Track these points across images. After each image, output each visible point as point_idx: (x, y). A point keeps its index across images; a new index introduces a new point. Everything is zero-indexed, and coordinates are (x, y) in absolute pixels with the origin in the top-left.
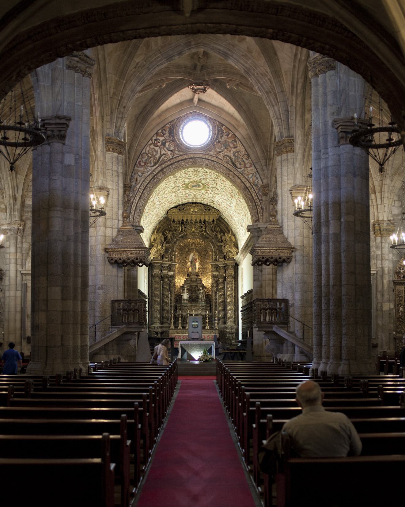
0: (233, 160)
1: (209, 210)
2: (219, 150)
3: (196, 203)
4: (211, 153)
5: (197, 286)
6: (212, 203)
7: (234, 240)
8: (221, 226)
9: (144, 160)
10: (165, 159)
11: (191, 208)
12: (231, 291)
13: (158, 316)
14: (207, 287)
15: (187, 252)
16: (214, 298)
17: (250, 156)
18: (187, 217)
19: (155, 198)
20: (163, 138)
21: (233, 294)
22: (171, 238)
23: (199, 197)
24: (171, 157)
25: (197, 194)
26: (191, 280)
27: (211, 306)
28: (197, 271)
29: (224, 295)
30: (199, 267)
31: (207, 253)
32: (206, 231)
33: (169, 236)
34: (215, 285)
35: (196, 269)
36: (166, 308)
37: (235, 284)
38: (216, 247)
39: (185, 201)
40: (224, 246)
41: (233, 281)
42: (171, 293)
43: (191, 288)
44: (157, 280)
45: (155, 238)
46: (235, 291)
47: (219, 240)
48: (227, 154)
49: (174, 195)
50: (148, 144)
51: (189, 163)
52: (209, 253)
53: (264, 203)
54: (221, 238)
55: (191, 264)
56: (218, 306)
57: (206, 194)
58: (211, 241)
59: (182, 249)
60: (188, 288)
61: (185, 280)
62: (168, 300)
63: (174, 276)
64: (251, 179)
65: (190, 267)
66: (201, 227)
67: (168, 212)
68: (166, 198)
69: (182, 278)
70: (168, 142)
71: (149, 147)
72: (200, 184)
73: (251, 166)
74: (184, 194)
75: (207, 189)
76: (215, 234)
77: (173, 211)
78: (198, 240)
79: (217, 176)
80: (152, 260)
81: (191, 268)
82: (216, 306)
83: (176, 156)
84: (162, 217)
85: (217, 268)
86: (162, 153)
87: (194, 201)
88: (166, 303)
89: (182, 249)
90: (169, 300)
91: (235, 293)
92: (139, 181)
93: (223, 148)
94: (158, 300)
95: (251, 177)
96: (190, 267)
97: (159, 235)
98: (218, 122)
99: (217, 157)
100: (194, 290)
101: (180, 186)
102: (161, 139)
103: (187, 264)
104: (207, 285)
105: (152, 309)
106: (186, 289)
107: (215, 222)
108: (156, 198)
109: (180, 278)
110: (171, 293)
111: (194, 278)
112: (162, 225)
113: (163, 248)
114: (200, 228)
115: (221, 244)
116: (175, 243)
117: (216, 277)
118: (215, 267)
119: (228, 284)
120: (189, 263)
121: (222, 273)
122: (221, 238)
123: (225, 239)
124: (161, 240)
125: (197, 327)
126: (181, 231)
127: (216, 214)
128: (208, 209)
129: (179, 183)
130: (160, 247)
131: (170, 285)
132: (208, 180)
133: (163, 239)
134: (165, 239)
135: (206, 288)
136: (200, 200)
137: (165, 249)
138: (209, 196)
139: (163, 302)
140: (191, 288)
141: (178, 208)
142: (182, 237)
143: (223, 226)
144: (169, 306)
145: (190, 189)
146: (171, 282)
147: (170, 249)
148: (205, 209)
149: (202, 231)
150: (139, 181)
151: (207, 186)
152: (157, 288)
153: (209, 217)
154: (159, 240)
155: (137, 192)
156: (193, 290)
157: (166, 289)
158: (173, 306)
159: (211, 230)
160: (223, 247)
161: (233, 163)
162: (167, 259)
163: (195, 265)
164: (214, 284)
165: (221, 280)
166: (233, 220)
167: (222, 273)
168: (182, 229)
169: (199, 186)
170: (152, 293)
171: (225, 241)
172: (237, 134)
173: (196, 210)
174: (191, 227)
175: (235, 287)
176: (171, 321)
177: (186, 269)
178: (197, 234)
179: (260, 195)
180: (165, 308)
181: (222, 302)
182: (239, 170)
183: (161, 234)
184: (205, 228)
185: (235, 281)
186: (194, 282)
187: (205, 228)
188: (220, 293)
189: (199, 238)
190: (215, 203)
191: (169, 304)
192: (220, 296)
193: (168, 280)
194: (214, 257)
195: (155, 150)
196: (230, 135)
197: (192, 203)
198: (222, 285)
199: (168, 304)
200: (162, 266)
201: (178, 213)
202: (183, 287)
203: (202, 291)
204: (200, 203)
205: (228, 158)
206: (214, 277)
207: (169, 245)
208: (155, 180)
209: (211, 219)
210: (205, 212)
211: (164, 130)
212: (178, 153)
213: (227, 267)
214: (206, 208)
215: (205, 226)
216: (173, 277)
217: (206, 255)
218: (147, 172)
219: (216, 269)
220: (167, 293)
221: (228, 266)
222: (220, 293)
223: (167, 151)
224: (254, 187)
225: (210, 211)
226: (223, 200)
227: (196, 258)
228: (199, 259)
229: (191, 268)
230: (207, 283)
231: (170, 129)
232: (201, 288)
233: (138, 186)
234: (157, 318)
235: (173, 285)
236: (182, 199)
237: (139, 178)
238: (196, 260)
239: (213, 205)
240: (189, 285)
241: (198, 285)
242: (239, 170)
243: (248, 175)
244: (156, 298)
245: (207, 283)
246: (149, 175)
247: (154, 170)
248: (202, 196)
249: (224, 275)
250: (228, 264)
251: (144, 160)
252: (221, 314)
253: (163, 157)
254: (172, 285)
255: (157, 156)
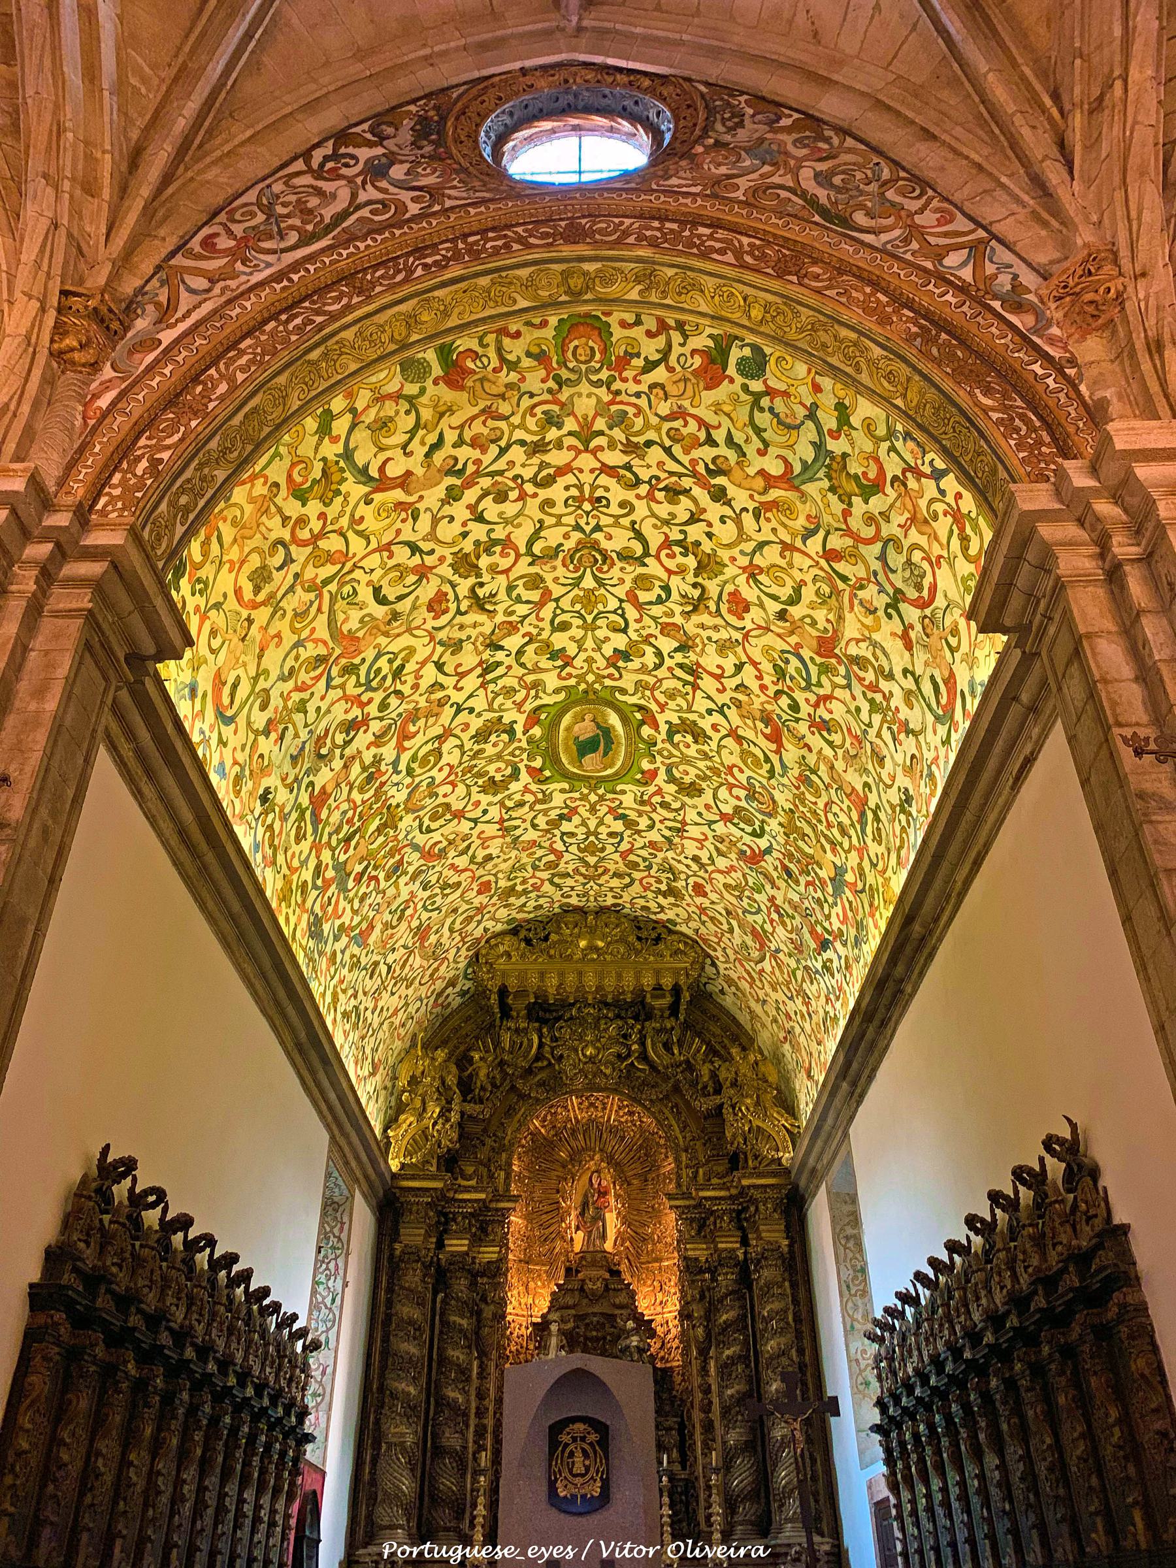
0: (823, 200)
1: (658, 940)
2: (723, 170)
3: (601, 911)
4: (674, 181)
5: (611, 1318)
6: (671, 892)
7: (773, 1078)
8: (708, 1030)
9: (238, 229)
10: (377, 218)
11: (579, 936)
12: (782, 1332)
13: (407, 1485)
14: (660, 1331)
15: (564, 1167)
16: (697, 1381)
17: (930, 175)
18: (561, 975)
19: (388, 752)
20: (379, 151)
21: (794, 1352)
22: (494, 1085)
23: (614, 862)
24: (414, 209)
25: (603, 830)
26: (582, 1290)
27: (682, 1427)
28: (608, 1246)
29: (743, 1358)
30: (619, 1232)
31: (655, 1166)
32: (644, 1057)
33: (483, 1073)
34: (698, 1311)
35: (604, 1237)
36: (451, 1439)
37: (795, 1301)
38: (693, 1126)
39: (551, 898)
40: (733, 1107)
41: (787, 1284)
42: (483, 1355)
43: (582, 1330)
44: (413, 1278)
45: (418, 1073)
46: (799, 1335)
47: (705, 1087)
48: (776, 179)
49: (494, 813)
50: (281, 174)
51: (532, 240)
52: (659, 1167)
53: (1091, 373)
54: (714, 1075)
55: (582, 1214)
56: (717, 1424)
57: (644, 823)
58: (667, 1097)
59: (543, 1149)
60: (570, 1325)
61: (553, 1294)
62: (466, 1393)
63: (499, 1268)
64: (967, 274)
65: (578, 1228)
66: (625, 1036)
67: (477, 955)
68: (459, 815)
69: (544, 1286)
70: (402, 162)
71: (286, 184)
72: (614, 720)
73: (944, 220)
74: (541, 821)
75: (646, 765)
76: (687, 1062)
77: (501, 949)
78: (614, 1101)
79: (699, 570)
80: (394, 1176)
81: (581, 1234)
82: (708, 1427)
83: (449, 203)
84: (452, 983)
85: (702, 1227)
86: (363, 197)
87: (592, 904)
88: (453, 1407)
89: (543, 1149)
90: (473, 1393)
91: (801, 1352)
92: (179, 314)
93: (747, 163)
94: (412, 1390)
95: (964, 264)
96: (578, 1228)
97: (433, 1059)
98: (707, 84)
99: (714, 196)
100: (597, 1339)
101: (519, 728)
102: (364, 153)
103: (563, 1220)
104: (659, 1318)
105: (380, 1448)
106: (554, 1328)
107: (686, 996)
108: (395, 763)
109: (532, 1285)
110: (483, 1355)
111: (594, 1279)
112: (456, 1030)
113: (448, 1120)
114: (618, 1042)
115: (718, 1100)
116: (510, 1112)
117: (701, 1271)
118: (692, 1220)
119: (761, 1297)
120: (574, 1214)
121: (729, 1243)
122: (714, 1075)
123: (731, 1076)
124: (443, 1083)
125: (605, 1497)
126: (539, 1057)
127: (684, 963)
128: (654, 935)
129: (509, 692)
130: (434, 1110)
131: (479, 1313)
132: (650, 659)
133: (451, 1080)
134: (466, 1086)
135: (653, 1334)
136: (615, 883)
137: (460, 1125)
138: (654, 836)
139: (442, 1403)
140: (582, 1330)
141: (523, 934)
142: (542, 1084)
143: (718, 1031)
144: (472, 1429)
145: (566, 776)
146: (484, 1299)
147: (489, 1142)
148: (639, 939)
149: (629, 1055)
150: (179, 314)
151: (646, 731)
152: (411, 1322)
153: (658, 973)
154: (434, 1079)
155: (157, 361)
156: (591, 1339)
157: (461, 1331)
158: (490, 1429)
159: (667, 1046)
160: (727, 1111)
161: (824, 212)
162: (473, 1183)
163: (599, 1217)
164: (694, 1306)
165: (727, 1279)
166: (767, 965)
167: (729, 1243)
168: (541, 1045)
169: (607, 732)
170: (386, 1353)
171: (734, 1084)
172: (830, 106)
173: (600, 944)
174: (581, 1039)
175: (797, 1319)
176: (472, 1526)
177: (558, 1244)
178: (608, 1072)
179: (1052, 341)
180: (445, 1442)
181: (741, 1400)
182: (869, 238)
183: (441, 1055)
184: (642, 1043)
185: (794, 1286)
186: (594, 1298)
187: (642, 1043)
188: (727, 1352)
189: (615, 1091)
190: (680, 884)
191: (473, 1422)
192: (725, 1365)
193: (473, 1285)
194: (686, 1174)
195: (319, 192)
196: (785, 122)
197: (581, 911)
198: (732, 1308)
199: (465, 1414)
200: (445, 1215)
201: (523, 956)
202: (541, 1328)
203: (634, 1341)
204: (616, 910)
205: (784, 194)
206: (690, 1268)
207: (478, 1108)
208: (298, 321)
209: (667, 982)
210: (638, 953)
211: (390, 124)
212: (464, 195)
213: (752, 1209)
214: (644, 934)
215: (640, 1032)
216: (496, 1271)
217: (650, 1177)
218: (251, 274)
219: (699, 1232)
220: (456, 1354)
221: (753, 1201)
222: (727, 1352)
223: (392, 189)
224: (996, 305)
225: (661, 946)
226: (720, 828)
227: (604, 1183)
228: (617, 1196)
229: (581, 1234)
230: (659, 1309)
231: (423, 120)
232: (630, 1324)
233: (167, 337)
234: (395, 1498)
235: (495, 1315)
236: (535, 868)
237: (185, 301)
238: (603, 1193)
239: (670, 915)
240: (573, 1312)
241: (617, 1312)
242: (869, 238)
243: (940, 258)
244: (399, 1379)
245: (659, 1309)
246: (261, 284)
247: (295, 267)
248: (624, 846)
249: (740, 1254)
250: (757, 1194)
251: (238, 229)
252: (741, 1479)
253: (365, 212)
254: (488, 1311)
255: (328, 213)
